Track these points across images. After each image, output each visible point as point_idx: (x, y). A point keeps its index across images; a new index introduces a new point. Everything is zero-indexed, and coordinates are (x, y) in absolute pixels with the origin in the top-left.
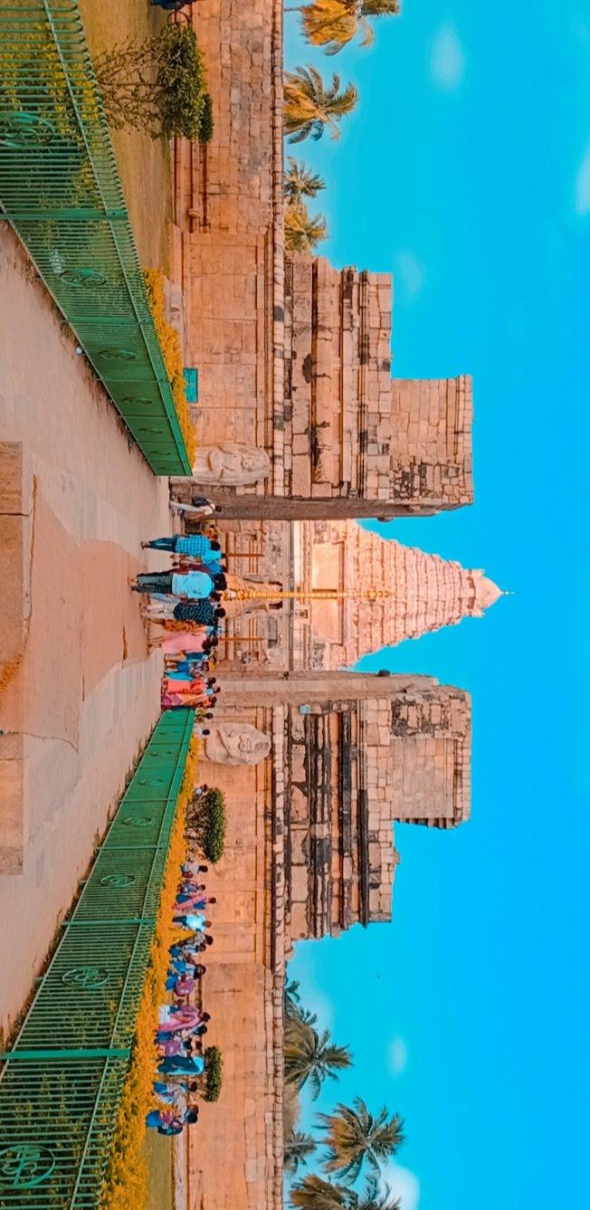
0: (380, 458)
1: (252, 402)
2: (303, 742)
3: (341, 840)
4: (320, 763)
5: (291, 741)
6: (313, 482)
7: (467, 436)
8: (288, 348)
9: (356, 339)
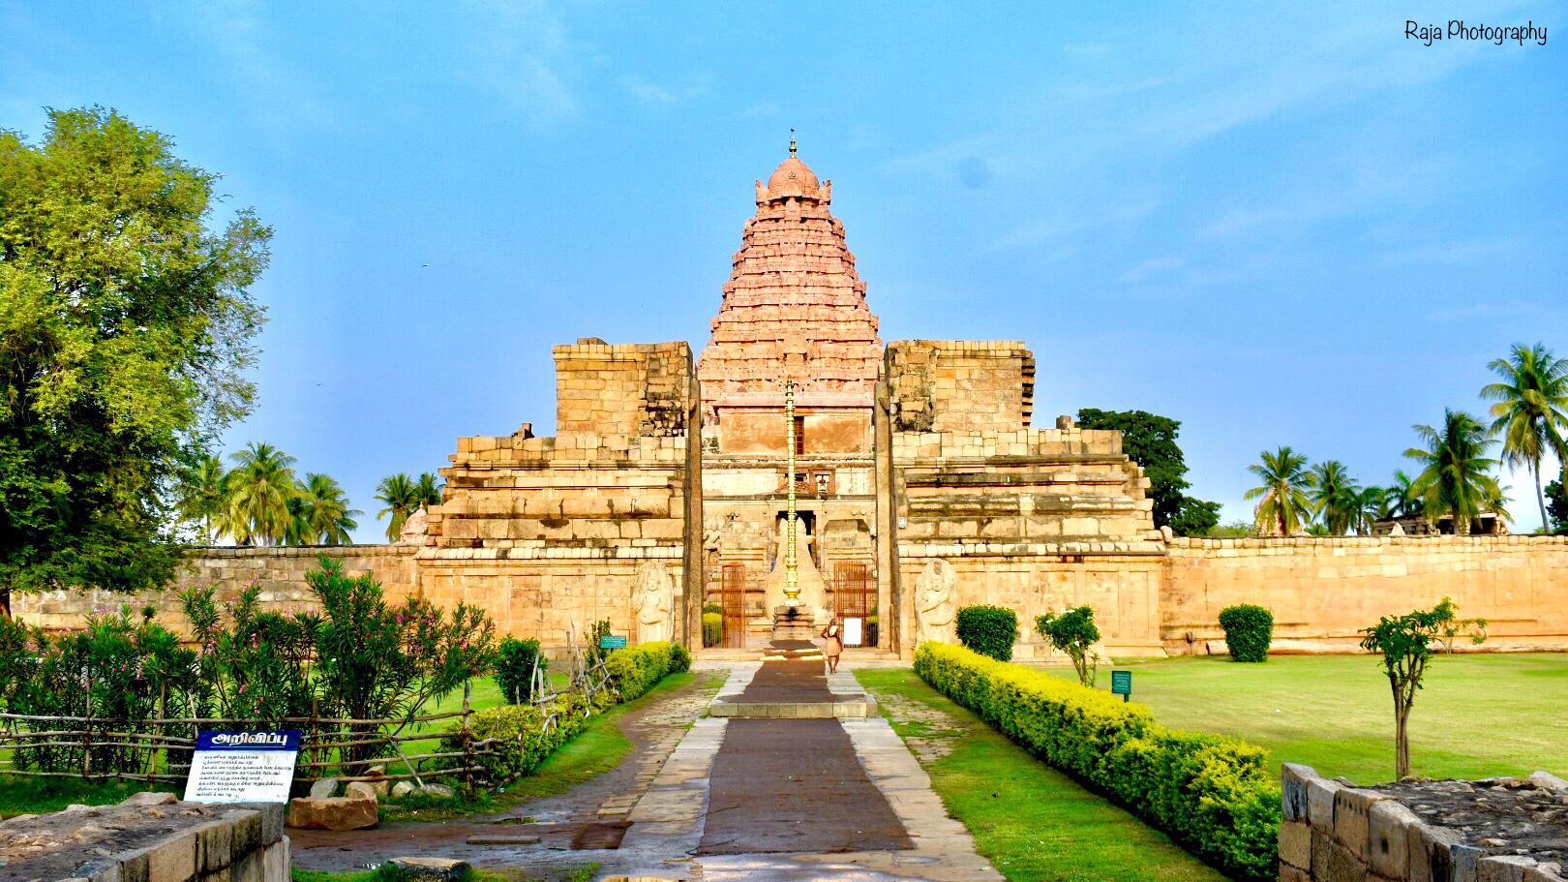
0: (644, 447)
1: (590, 580)
2: (937, 524)
3: (1039, 484)
4: (959, 507)
5: (937, 538)
6: (669, 516)
7: (616, 349)
8: (534, 543)
9: (522, 473)
